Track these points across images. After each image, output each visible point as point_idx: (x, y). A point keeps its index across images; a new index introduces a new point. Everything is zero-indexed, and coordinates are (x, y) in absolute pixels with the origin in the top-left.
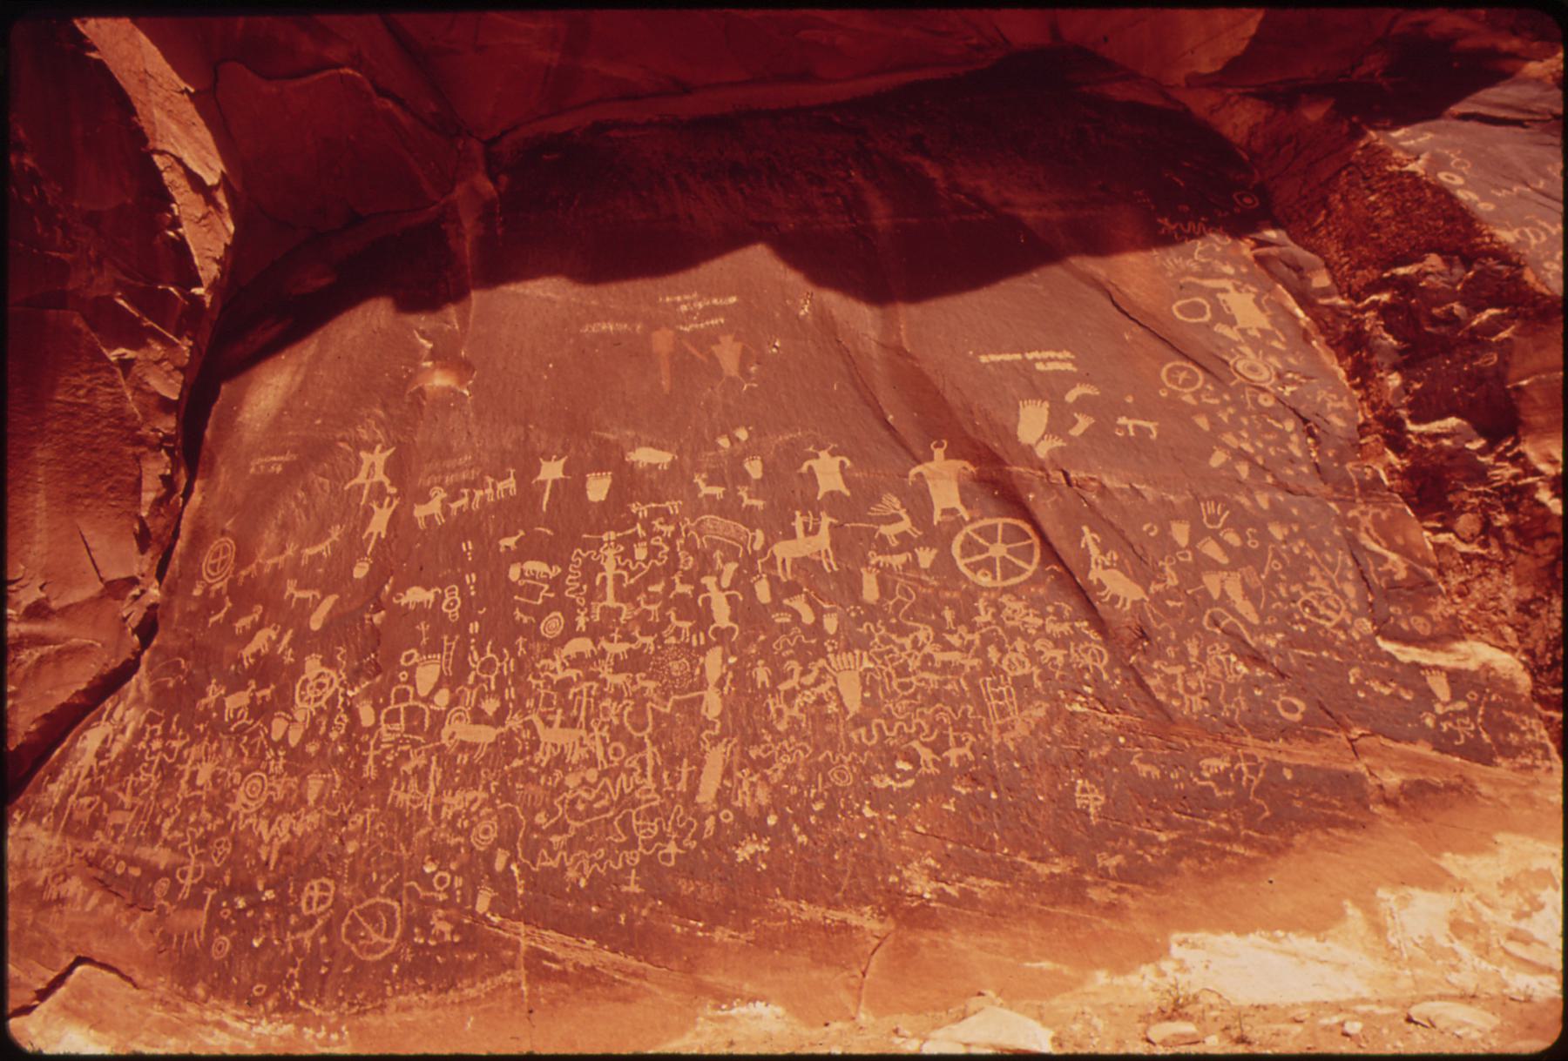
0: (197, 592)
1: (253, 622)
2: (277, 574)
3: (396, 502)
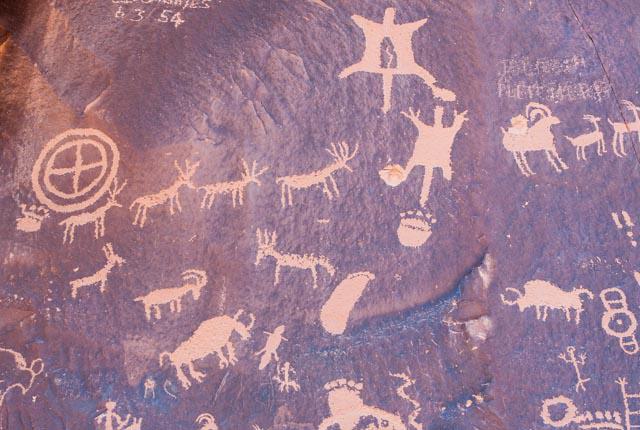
0: (29, 223)
1: (186, 299)
2: (227, 216)
3: (460, 119)
